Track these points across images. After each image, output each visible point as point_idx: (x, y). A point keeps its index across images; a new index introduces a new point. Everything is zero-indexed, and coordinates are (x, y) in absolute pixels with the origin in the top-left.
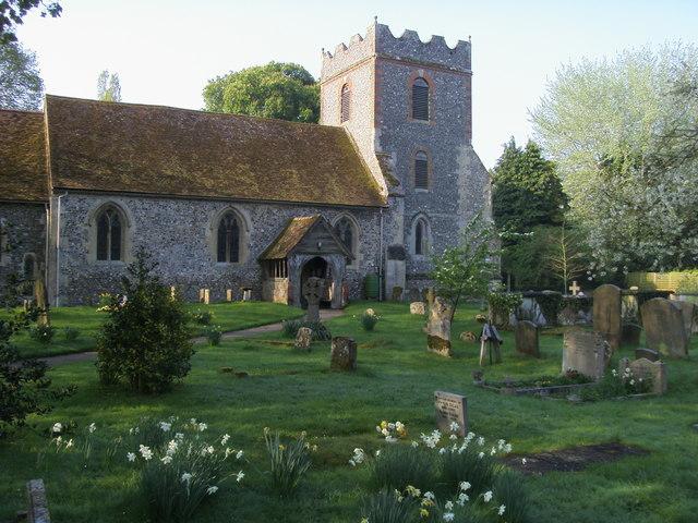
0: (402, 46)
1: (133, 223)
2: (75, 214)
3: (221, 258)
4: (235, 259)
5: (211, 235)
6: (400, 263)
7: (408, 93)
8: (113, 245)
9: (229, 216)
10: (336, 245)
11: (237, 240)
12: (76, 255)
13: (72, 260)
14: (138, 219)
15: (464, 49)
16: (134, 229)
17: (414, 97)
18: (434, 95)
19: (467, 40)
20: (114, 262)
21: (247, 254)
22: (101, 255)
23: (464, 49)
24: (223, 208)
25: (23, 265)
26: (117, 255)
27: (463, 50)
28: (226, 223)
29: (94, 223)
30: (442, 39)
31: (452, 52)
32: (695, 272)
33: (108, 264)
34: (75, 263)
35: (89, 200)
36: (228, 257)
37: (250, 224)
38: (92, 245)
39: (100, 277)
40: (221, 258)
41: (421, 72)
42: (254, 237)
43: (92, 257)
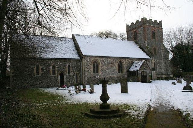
0: (149, 22)
1: (101, 64)
2: (88, 62)
3: (119, 72)
4: (122, 72)
5: (117, 66)
6: (154, 71)
7: (151, 33)
8: (95, 71)
9: (120, 62)
10: (147, 68)
11: (122, 67)
12: (88, 72)
13: (88, 73)
14: (102, 63)
15: (161, 22)
16: (101, 65)
17: (152, 34)
18: (156, 34)
19: (161, 21)
20: (97, 74)
21: (125, 71)
22: (94, 72)
23: (161, 22)
24: (119, 60)
25: (75, 75)
26: (97, 72)
27: (128, 26)
28: (120, 63)
29: (92, 64)
30: (156, 21)
31: (158, 23)
32: (192, 72)
33: (95, 74)
34: (89, 74)
35: (91, 58)
36: (120, 72)
37: (125, 64)
38: (92, 69)
39: (94, 77)
40: (119, 72)
41: (153, 28)
42: (126, 66)
43: (92, 72)
